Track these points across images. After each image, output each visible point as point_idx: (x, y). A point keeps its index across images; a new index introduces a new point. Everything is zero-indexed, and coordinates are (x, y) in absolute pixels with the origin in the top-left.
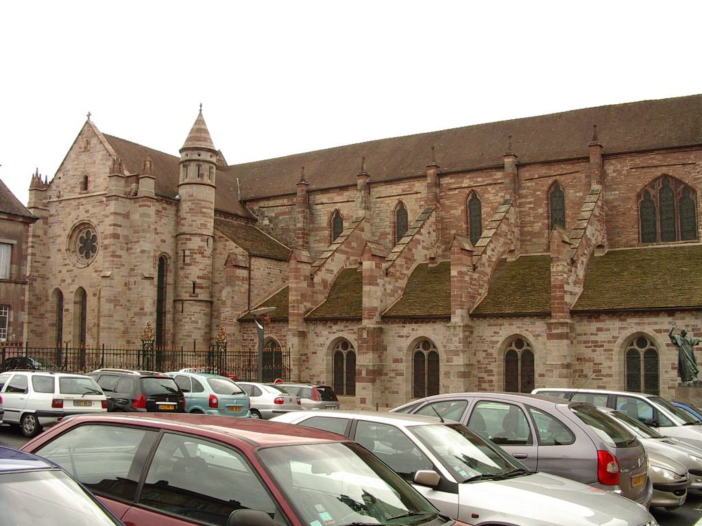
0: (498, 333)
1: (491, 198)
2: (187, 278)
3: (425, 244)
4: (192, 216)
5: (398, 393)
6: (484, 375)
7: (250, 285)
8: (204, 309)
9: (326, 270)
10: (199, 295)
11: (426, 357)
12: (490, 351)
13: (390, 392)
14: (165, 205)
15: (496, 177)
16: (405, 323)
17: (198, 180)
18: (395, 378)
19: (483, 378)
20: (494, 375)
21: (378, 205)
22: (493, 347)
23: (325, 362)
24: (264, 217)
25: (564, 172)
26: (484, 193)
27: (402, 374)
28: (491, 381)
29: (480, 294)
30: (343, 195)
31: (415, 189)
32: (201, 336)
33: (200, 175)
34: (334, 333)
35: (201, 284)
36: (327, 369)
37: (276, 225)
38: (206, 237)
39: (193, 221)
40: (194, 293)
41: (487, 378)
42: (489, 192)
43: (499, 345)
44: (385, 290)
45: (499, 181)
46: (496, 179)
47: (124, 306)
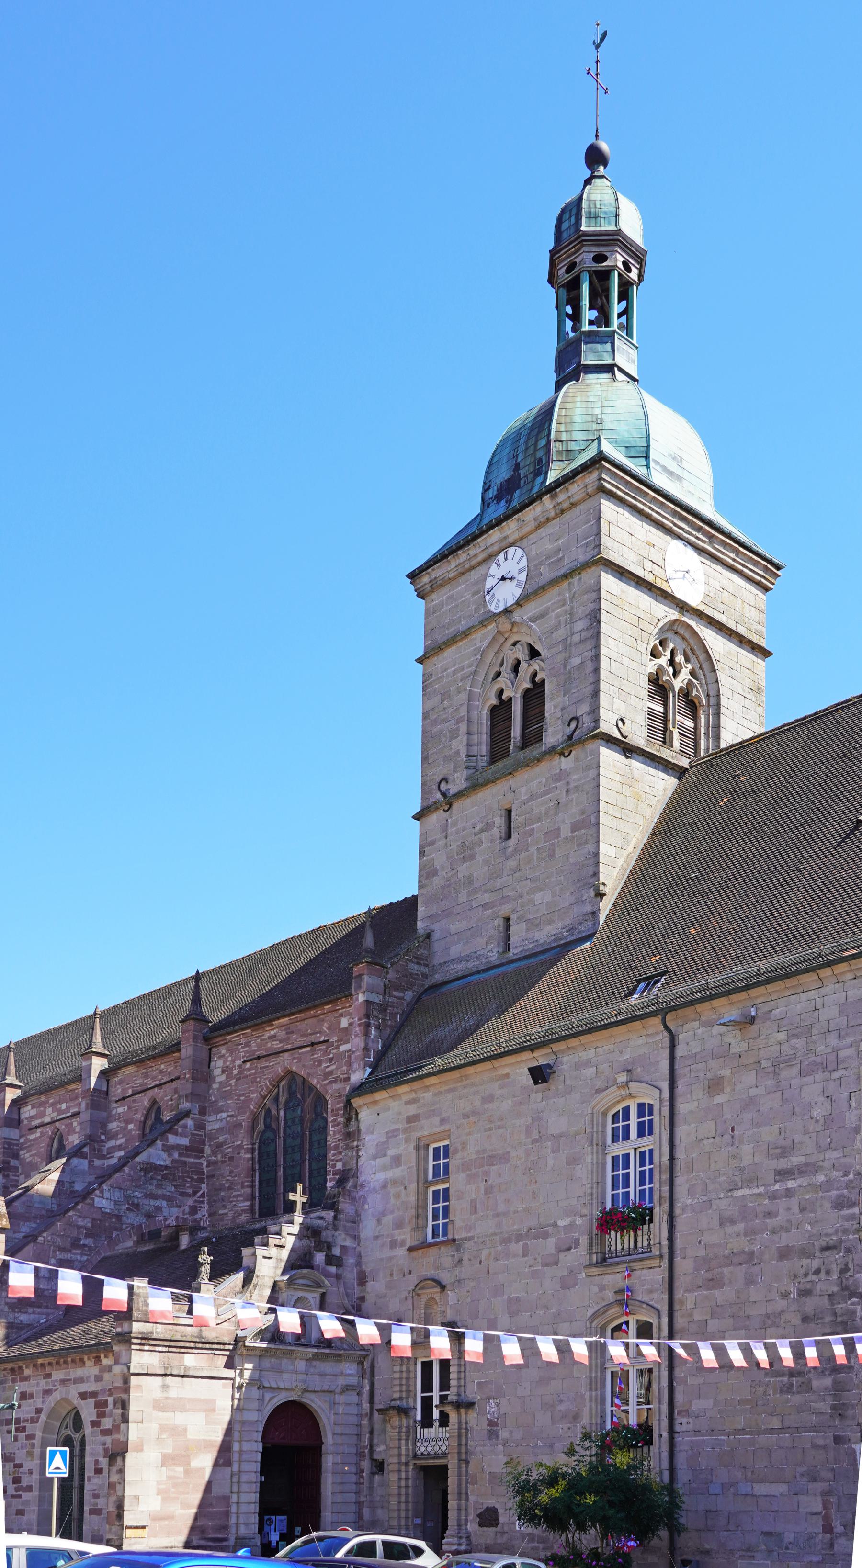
25: (165, 1079)
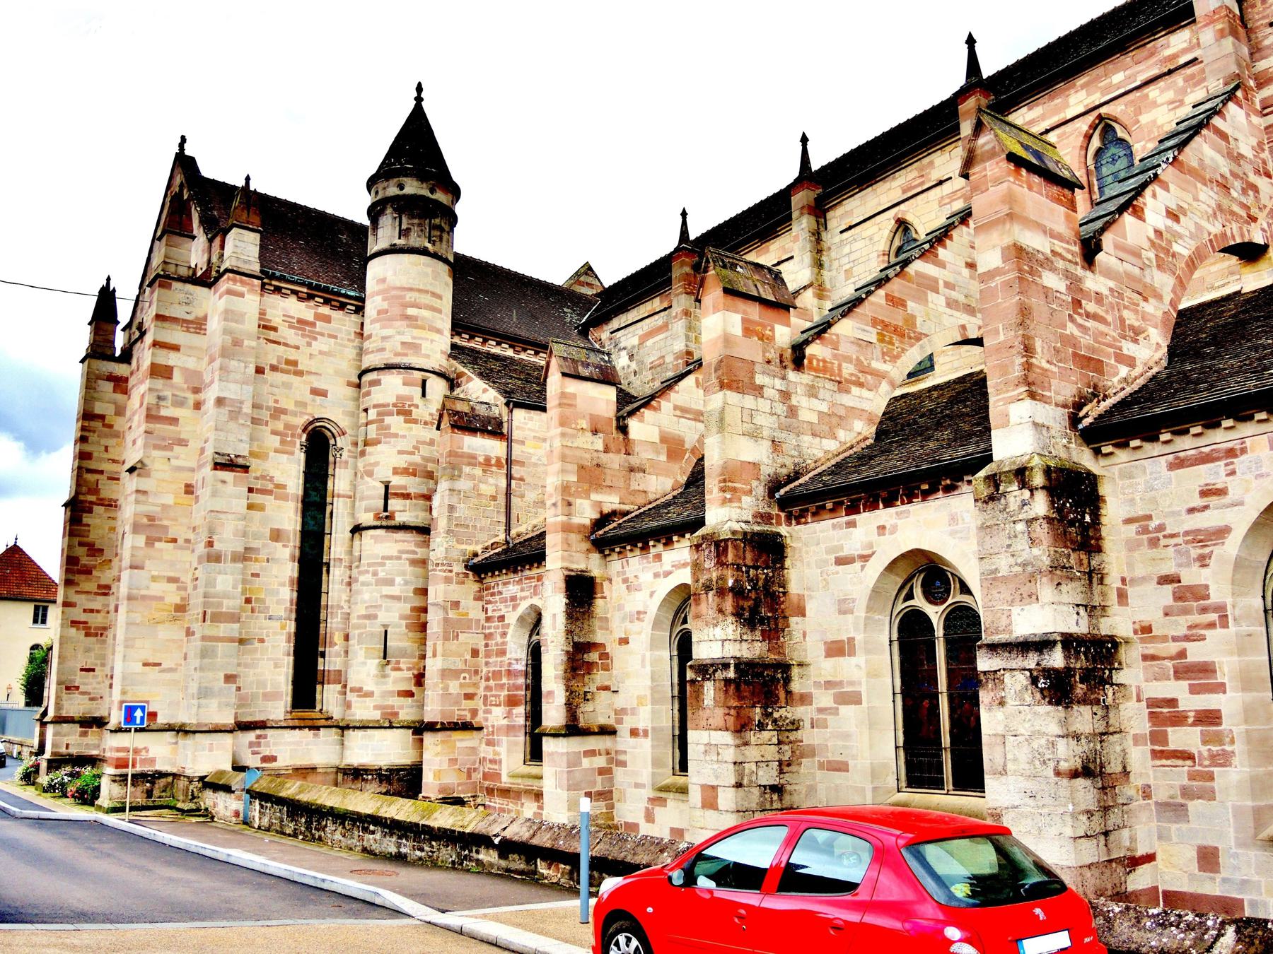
0: (1221, 492)
1: (1160, 122)
2: (370, 474)
3: (954, 295)
4: (382, 327)
5: (841, 767)
6: (1178, 690)
7: (509, 477)
8: (413, 548)
9: (676, 408)
10: (397, 515)
11: (939, 632)
12: (1192, 576)
13: (821, 766)
14: (325, 310)
15: (1167, 52)
16: (853, 510)
17: (401, 242)
18: (835, 712)
19: (1172, 702)
20: (1221, 688)
21: (846, 250)
22: (1203, 560)
23: (648, 669)
24: (620, 350)
26: (1138, 112)
27: (855, 699)
28: (1209, 718)
29: (1130, 362)
30: (768, 251)
31: (935, 176)
32: (402, 617)
33: (403, 233)
34: (667, 574)
35: (405, 487)
36: (654, 689)
37: (641, 363)
38: (418, 375)
39: (384, 338)
40: (386, 509)
41: (1190, 703)
42: (1154, 104)
43: (1231, 547)
44: (792, 412)
45: (1182, 61)
46: (1175, 57)
47: (180, 541)
